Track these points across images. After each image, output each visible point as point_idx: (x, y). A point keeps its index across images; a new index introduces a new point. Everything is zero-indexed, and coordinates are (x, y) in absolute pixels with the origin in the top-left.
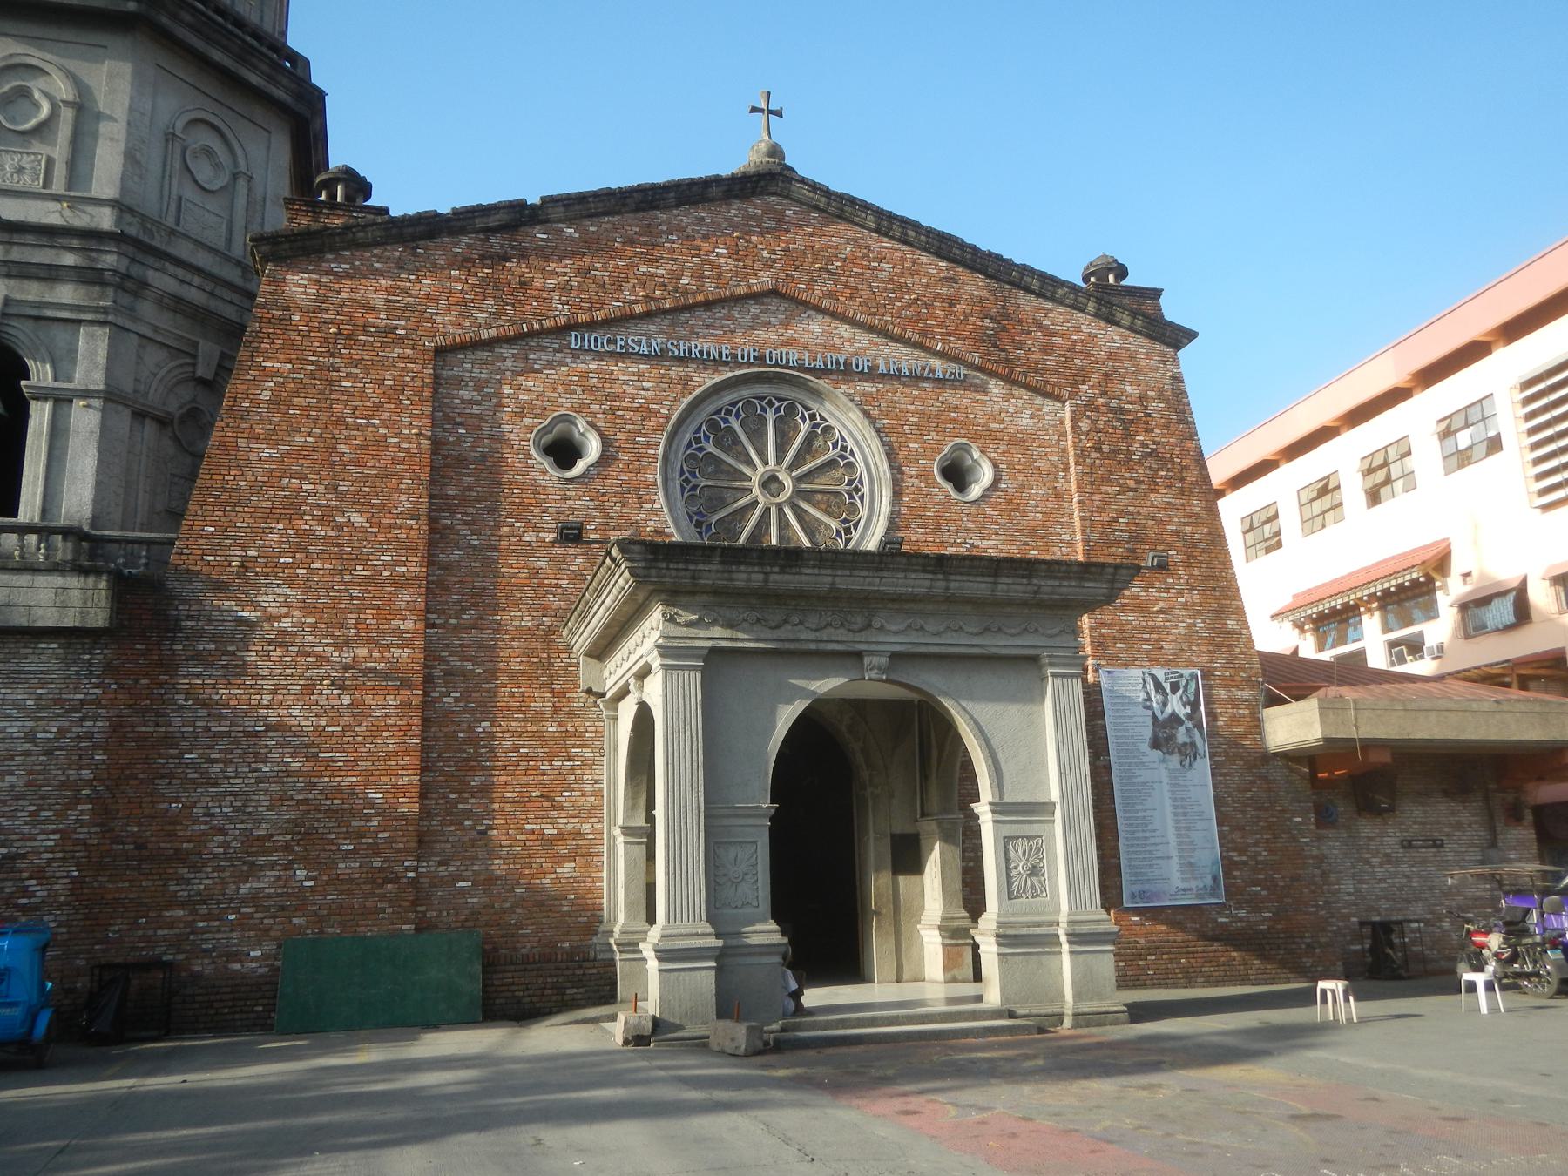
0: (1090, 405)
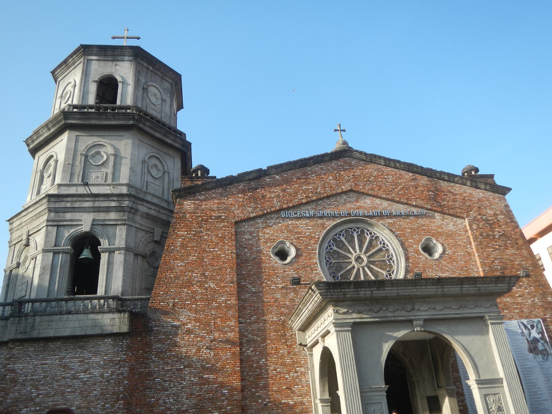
0: (475, 219)
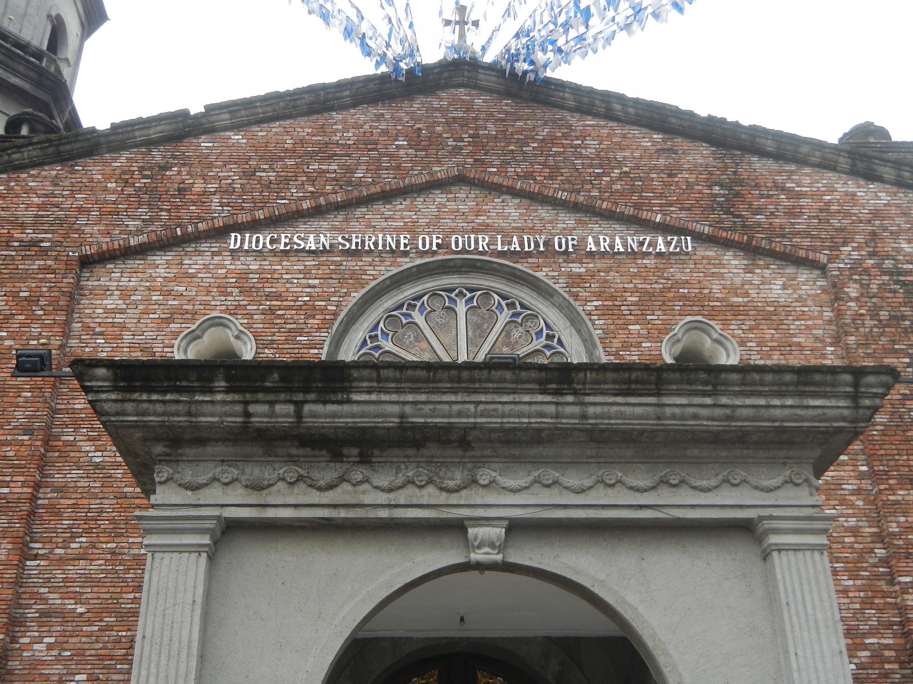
0: (856, 268)
